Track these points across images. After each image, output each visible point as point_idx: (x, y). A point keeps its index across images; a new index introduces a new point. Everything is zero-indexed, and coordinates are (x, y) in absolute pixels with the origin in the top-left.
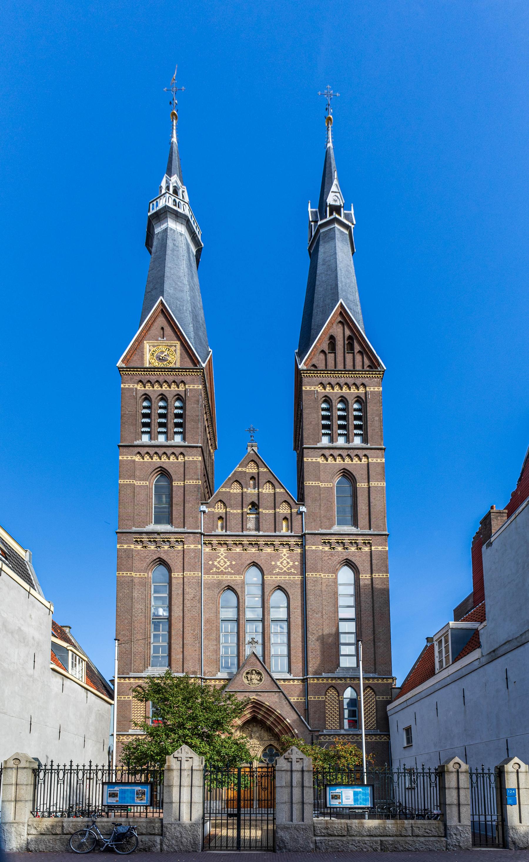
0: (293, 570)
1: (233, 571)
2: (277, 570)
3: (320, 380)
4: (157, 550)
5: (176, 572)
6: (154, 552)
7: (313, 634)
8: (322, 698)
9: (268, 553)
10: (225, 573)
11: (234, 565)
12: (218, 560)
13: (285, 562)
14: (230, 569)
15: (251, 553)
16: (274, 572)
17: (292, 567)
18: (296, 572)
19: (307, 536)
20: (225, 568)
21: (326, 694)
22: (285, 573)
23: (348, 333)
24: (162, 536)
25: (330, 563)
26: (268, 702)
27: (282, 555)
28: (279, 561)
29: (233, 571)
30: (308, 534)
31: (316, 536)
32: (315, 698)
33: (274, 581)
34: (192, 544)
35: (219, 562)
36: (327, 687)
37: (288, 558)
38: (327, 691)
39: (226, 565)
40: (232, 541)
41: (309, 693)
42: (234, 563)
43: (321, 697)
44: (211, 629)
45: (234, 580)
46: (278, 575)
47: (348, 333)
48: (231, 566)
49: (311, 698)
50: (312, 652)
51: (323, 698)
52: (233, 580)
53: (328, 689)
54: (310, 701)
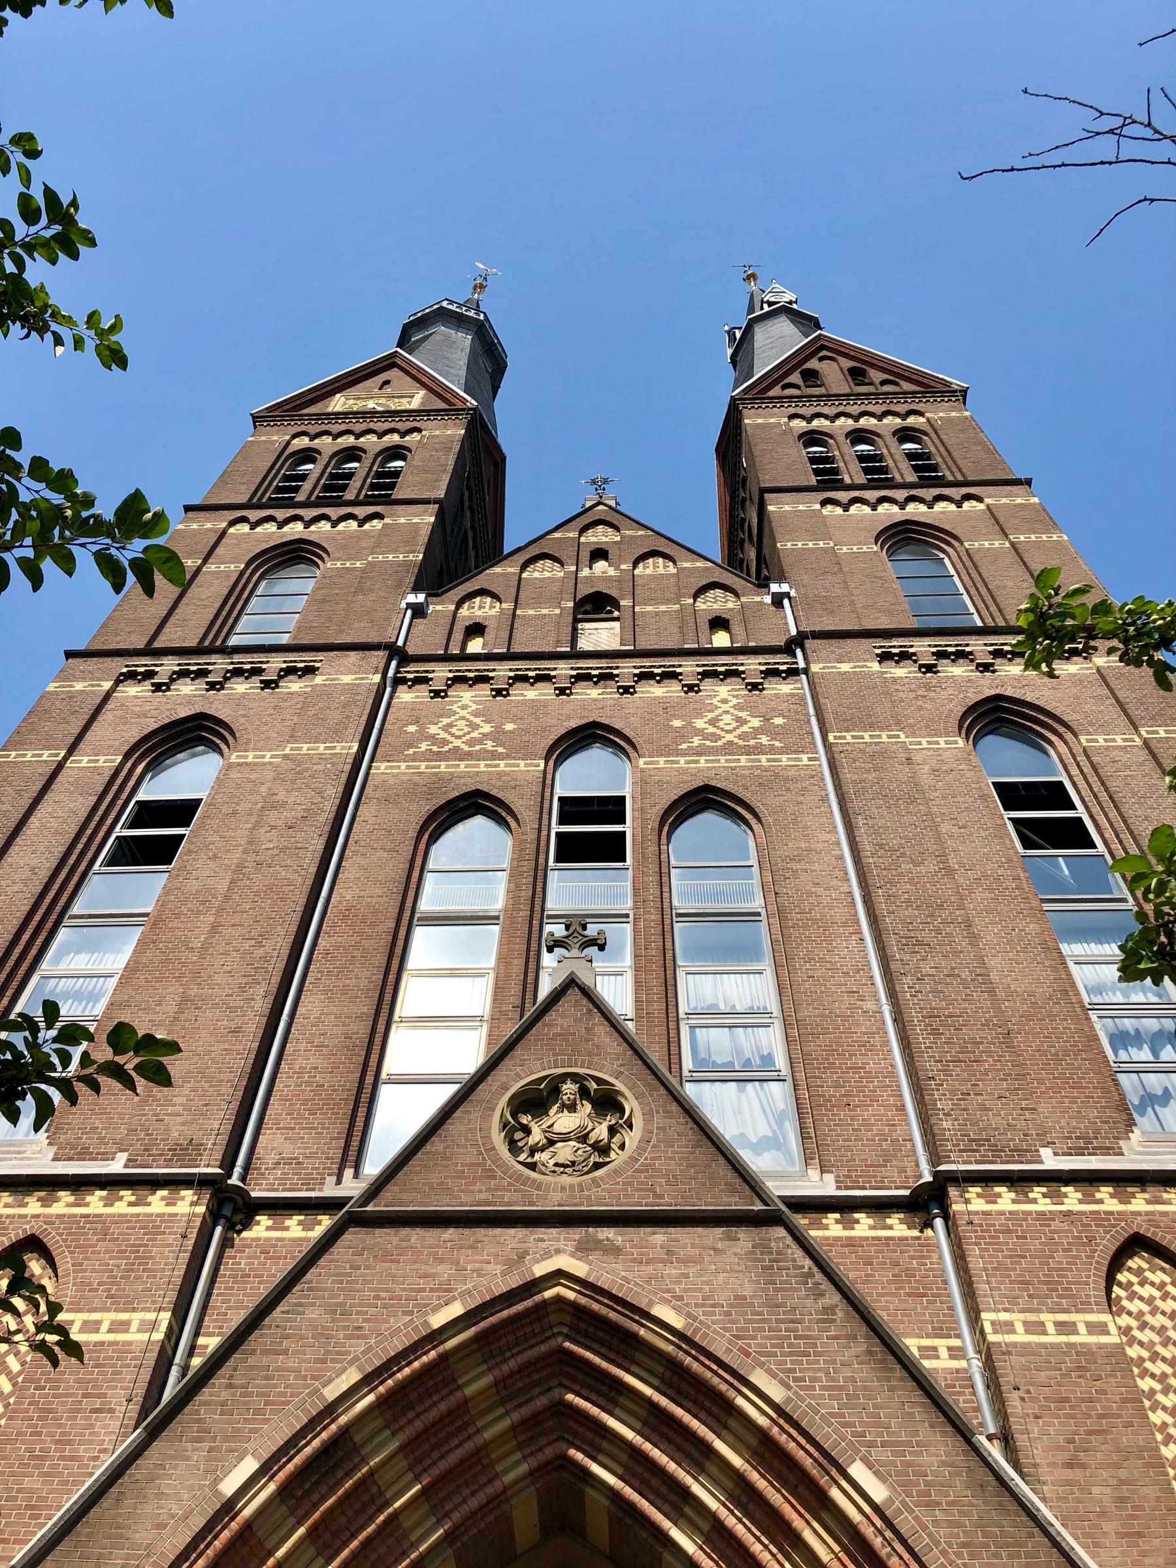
0: (764, 740)
1: (500, 750)
2: (696, 741)
3: (792, 411)
4: (201, 695)
5: (254, 750)
6: (189, 700)
7: (919, 943)
8: (1092, 1329)
9: (655, 698)
10: (469, 756)
11: (511, 732)
12: (445, 721)
13: (727, 718)
14: (489, 745)
15: (585, 700)
16: (684, 746)
17: (757, 731)
18: (777, 744)
19: (809, 644)
20: (471, 743)
21: (1111, 1304)
22: (729, 749)
23: (847, 364)
24: (237, 658)
25: (929, 706)
26: (676, 1301)
27: (715, 701)
28: (700, 715)
29: (500, 750)
30: (816, 635)
31: (849, 642)
32: (1040, 1328)
33: (684, 771)
34: (350, 672)
35: (451, 725)
36: (1107, 1245)
37: (741, 709)
38: (1110, 1280)
39: (473, 735)
40: (511, 670)
41: (981, 1288)
42: (509, 727)
43: (1079, 1319)
44: (356, 946)
45: (501, 774)
46: (700, 754)
47: (847, 364)
48: (497, 736)
49: (1008, 1327)
50: (936, 1033)
51: (1102, 1329)
52: (498, 773)
53: (1116, 1263)
54: (1009, 1350)
